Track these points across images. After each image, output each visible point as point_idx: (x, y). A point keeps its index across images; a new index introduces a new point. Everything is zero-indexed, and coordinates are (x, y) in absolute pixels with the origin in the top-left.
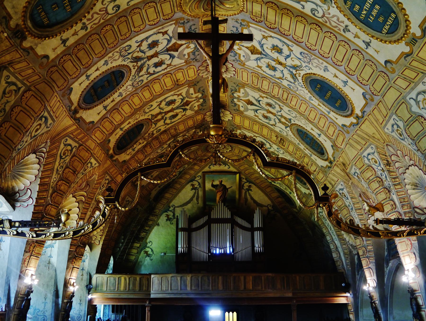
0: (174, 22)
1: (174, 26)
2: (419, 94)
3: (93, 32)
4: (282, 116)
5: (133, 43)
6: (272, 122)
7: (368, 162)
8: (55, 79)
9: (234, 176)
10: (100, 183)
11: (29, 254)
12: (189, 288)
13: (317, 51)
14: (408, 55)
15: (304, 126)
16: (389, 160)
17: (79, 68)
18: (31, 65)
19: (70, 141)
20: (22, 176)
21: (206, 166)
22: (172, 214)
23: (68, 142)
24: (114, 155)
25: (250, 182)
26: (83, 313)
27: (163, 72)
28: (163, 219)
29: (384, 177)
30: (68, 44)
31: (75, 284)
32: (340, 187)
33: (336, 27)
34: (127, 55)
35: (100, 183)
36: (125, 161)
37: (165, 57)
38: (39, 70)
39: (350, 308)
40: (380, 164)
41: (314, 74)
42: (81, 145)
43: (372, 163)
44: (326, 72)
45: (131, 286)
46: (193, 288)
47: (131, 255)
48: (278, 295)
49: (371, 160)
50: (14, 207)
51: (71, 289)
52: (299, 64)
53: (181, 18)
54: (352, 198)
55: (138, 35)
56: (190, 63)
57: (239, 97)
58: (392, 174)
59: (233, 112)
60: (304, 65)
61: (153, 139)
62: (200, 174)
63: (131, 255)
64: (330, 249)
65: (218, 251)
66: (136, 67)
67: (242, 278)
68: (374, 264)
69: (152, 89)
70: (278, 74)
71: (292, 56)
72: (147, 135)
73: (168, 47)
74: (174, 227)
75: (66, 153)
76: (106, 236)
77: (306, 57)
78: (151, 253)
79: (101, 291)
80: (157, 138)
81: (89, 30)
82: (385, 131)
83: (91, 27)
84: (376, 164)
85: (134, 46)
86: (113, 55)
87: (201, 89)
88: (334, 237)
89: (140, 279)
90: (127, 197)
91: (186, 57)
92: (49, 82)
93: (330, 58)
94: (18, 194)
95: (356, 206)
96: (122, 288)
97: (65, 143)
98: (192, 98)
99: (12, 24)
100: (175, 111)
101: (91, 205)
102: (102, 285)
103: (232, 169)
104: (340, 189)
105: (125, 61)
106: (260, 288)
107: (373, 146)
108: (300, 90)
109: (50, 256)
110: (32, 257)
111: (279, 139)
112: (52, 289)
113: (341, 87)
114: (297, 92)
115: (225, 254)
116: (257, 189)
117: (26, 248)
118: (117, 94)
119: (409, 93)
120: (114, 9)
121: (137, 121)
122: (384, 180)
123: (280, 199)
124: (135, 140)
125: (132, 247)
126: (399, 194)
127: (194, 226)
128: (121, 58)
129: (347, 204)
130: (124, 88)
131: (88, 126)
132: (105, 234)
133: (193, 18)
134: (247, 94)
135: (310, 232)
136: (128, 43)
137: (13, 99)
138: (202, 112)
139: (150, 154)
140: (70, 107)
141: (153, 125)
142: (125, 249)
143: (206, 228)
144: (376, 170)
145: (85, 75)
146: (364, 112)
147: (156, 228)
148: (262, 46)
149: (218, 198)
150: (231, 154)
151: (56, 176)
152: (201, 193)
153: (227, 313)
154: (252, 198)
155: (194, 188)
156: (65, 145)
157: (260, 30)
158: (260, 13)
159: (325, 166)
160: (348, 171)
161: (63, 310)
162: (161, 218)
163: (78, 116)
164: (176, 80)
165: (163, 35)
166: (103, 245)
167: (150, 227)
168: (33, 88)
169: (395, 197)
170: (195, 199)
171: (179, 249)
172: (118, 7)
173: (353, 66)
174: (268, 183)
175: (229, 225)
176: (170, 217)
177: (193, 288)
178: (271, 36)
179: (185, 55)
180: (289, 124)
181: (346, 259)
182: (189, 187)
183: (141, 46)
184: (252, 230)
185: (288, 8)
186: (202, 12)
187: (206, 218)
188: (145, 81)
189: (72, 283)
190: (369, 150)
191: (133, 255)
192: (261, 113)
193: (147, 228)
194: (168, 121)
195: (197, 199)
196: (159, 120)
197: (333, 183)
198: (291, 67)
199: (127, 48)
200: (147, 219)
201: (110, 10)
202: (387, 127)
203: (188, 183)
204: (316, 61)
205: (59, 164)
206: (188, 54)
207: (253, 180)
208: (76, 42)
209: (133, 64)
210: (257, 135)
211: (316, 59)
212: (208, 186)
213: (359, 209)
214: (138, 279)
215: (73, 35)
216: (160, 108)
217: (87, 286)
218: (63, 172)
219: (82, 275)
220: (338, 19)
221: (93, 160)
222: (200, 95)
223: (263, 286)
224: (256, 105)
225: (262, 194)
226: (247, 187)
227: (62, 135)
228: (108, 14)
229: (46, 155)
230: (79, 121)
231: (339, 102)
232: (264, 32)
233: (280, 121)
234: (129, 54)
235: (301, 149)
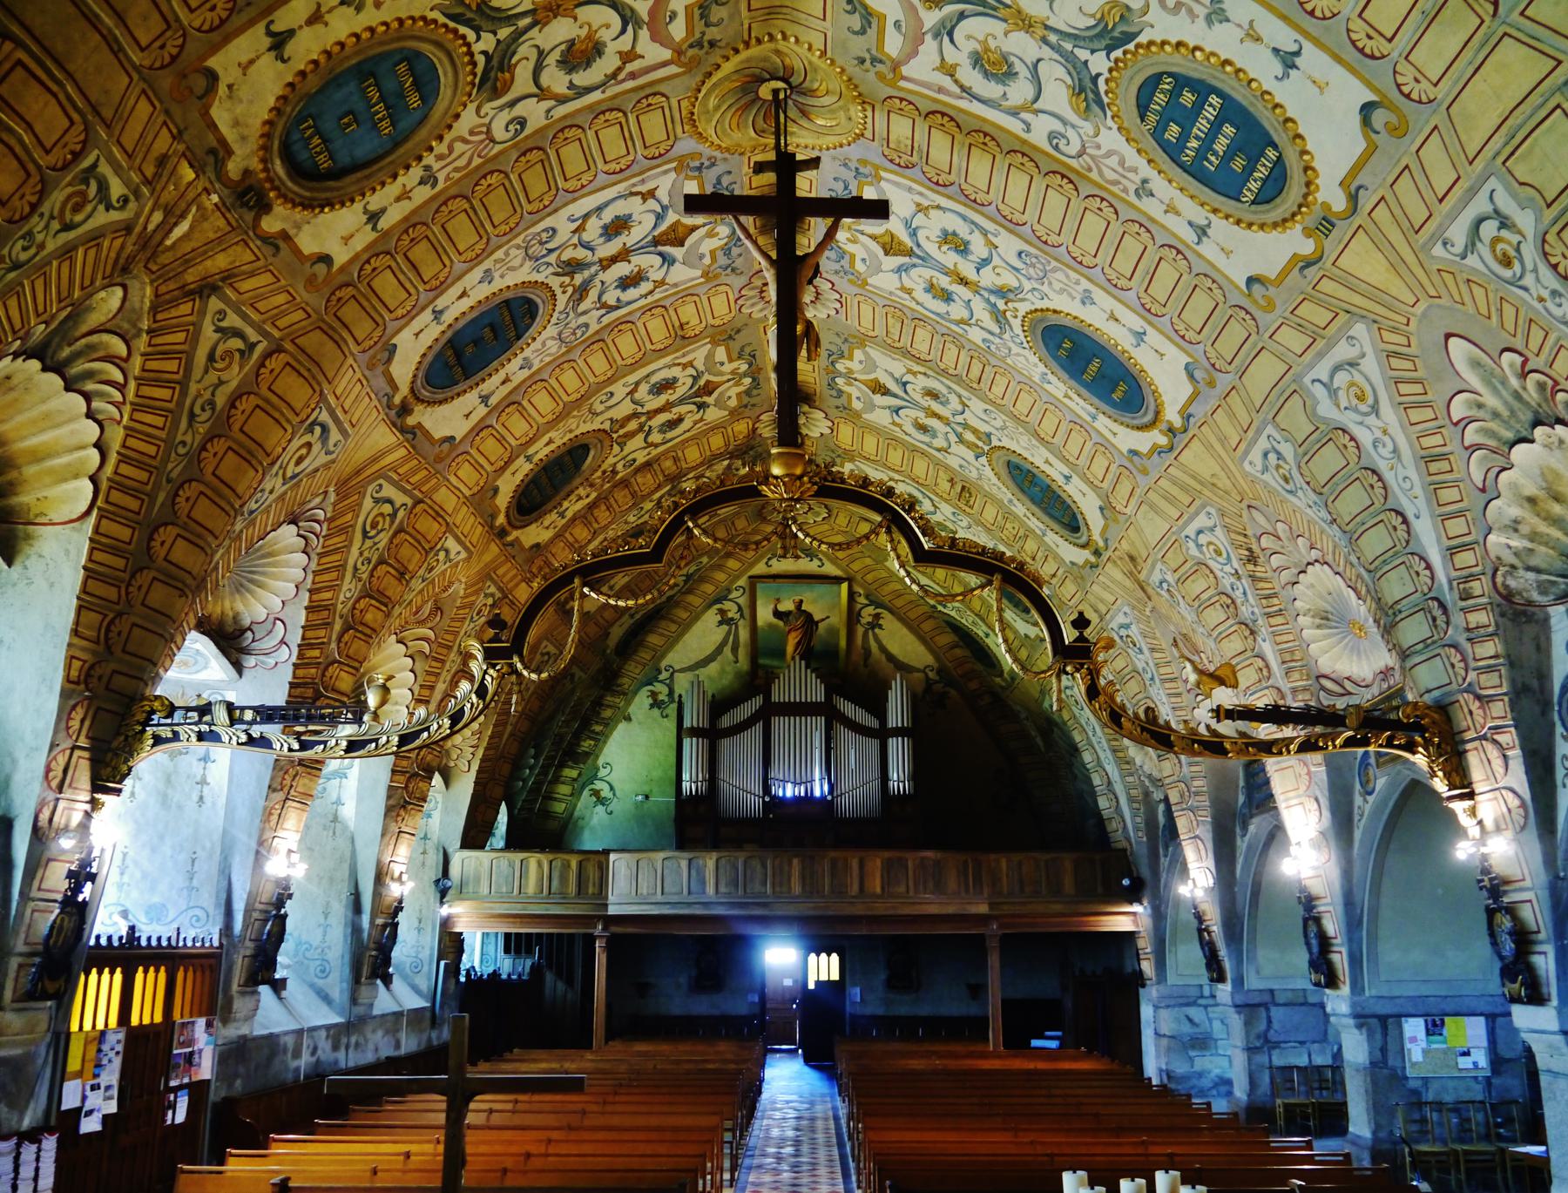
1: (673, 175)
2: (1337, 368)
3: (453, 192)
4: (966, 426)
5: (561, 222)
6: (939, 442)
7: (1197, 554)
8: (347, 320)
9: (835, 587)
10: (471, 605)
11: (280, 796)
12: (710, 890)
13: (1063, 249)
15: (1025, 454)
16: (1255, 547)
17: (412, 290)
19: (389, 491)
20: (260, 585)
21: (762, 557)
22: (665, 690)
23: (384, 494)
24: (508, 528)
25: (879, 605)
26: (427, 952)
27: (643, 302)
28: (641, 701)
29: (1238, 594)
30: (384, 223)
31: (405, 877)
32: (1121, 619)
33: (1117, 183)
35: (471, 605)
36: (537, 545)
37: (648, 261)
38: (306, 295)
39: (1141, 943)
40: (1229, 558)
41: (1055, 311)
42: (421, 501)
45: (555, 883)
46: (723, 889)
47: (556, 799)
48: (951, 910)
50: (239, 667)
51: (395, 890)
52: (1016, 284)
53: (692, 156)
54: (1152, 650)
55: (575, 200)
56: (716, 277)
57: (850, 371)
58: (1262, 585)
59: (833, 413)
60: (1027, 285)
61: (615, 486)
62: (742, 582)
63: (556, 799)
64: (1093, 787)
65: (790, 791)
66: (570, 289)
67: (855, 864)
68: (1209, 827)
69: (613, 349)
70: (957, 311)
71: (996, 261)
72: (599, 473)
73: (656, 233)
74: (671, 724)
76: (486, 749)
78: (610, 795)
79: (475, 897)
80: (625, 483)
81: (440, 186)
83: (447, 178)
84: (1219, 559)
85: (565, 229)
86: (507, 254)
87: (747, 350)
88: (1102, 756)
89: (580, 864)
90: (545, 643)
91: (707, 261)
92: (333, 329)
93: (1099, 269)
94: (249, 634)
95: (1162, 671)
96: (531, 887)
98: (722, 374)
100: (675, 410)
101: (447, 666)
102: (478, 880)
103: (830, 569)
104: (1122, 626)
106: (902, 889)
107: (1213, 511)
108: (1018, 355)
109: (339, 802)
110: (289, 803)
111: (958, 488)
112: (345, 891)
113: (1128, 347)
114: (1009, 361)
115: (808, 799)
116: (897, 625)
117: (272, 779)
118: (516, 363)
119: (1311, 366)
120: (511, 127)
121: (572, 436)
122: (1239, 601)
123: (958, 652)
124: (567, 489)
125: (557, 780)
126: (1279, 639)
127: (726, 721)
128: (528, 264)
129: (1140, 666)
130: (536, 345)
131: (437, 450)
132: (485, 744)
133: (726, 155)
134: (871, 365)
135: (1039, 741)
136: (548, 222)
137: (234, 376)
138: (747, 412)
139: (606, 527)
140: (390, 398)
141: (616, 448)
142: (538, 784)
143: (759, 727)
144: (1220, 574)
145: (430, 309)
146: (1190, 416)
147: (622, 727)
148: (914, 234)
149: (790, 649)
150: (826, 527)
151: (352, 586)
152: (744, 634)
153: (813, 956)
154: (883, 649)
155: (725, 620)
156: (377, 501)
157: (910, 190)
159: (1080, 562)
160: (1142, 577)
161: (372, 945)
162: (637, 699)
163: (411, 421)
164: (677, 324)
165: (645, 200)
166: (479, 772)
167: (606, 725)
168: (288, 346)
169: (1267, 648)
170: (727, 650)
171: (686, 785)
172: (522, 122)
173: (1160, 289)
174: (926, 609)
175: (821, 721)
176: (661, 697)
177: (723, 889)
178: (938, 207)
179: (702, 257)
180: (986, 448)
181: (1134, 816)
182: (711, 617)
184: (882, 734)
185: (987, 129)
186: (751, 139)
187: (758, 701)
188: (594, 327)
189: (396, 874)
190: (1201, 521)
191: (560, 801)
192: (909, 414)
193: (598, 728)
194: (656, 437)
195: (735, 650)
196: (631, 435)
197: (1103, 609)
198: (991, 292)
199: (544, 235)
200: (598, 704)
201: (499, 132)
202: (1250, 458)
203: (710, 606)
204: (1059, 275)
205: (361, 554)
206: (712, 253)
207: (886, 600)
208: (406, 219)
210: (897, 477)
212: (764, 615)
213: (1172, 680)
214: (574, 864)
215: (398, 199)
216: (634, 402)
217: (437, 882)
218: (372, 575)
219: (424, 853)
220: (1122, 163)
221: (451, 543)
222: (744, 367)
223: (911, 883)
224: (895, 396)
225: (910, 638)
226: (870, 619)
227: (369, 472)
228: (493, 141)
229: (325, 526)
230: (415, 434)
231: (1122, 387)
232: (921, 194)
233: (961, 440)
234: (550, 251)
235: (1016, 517)
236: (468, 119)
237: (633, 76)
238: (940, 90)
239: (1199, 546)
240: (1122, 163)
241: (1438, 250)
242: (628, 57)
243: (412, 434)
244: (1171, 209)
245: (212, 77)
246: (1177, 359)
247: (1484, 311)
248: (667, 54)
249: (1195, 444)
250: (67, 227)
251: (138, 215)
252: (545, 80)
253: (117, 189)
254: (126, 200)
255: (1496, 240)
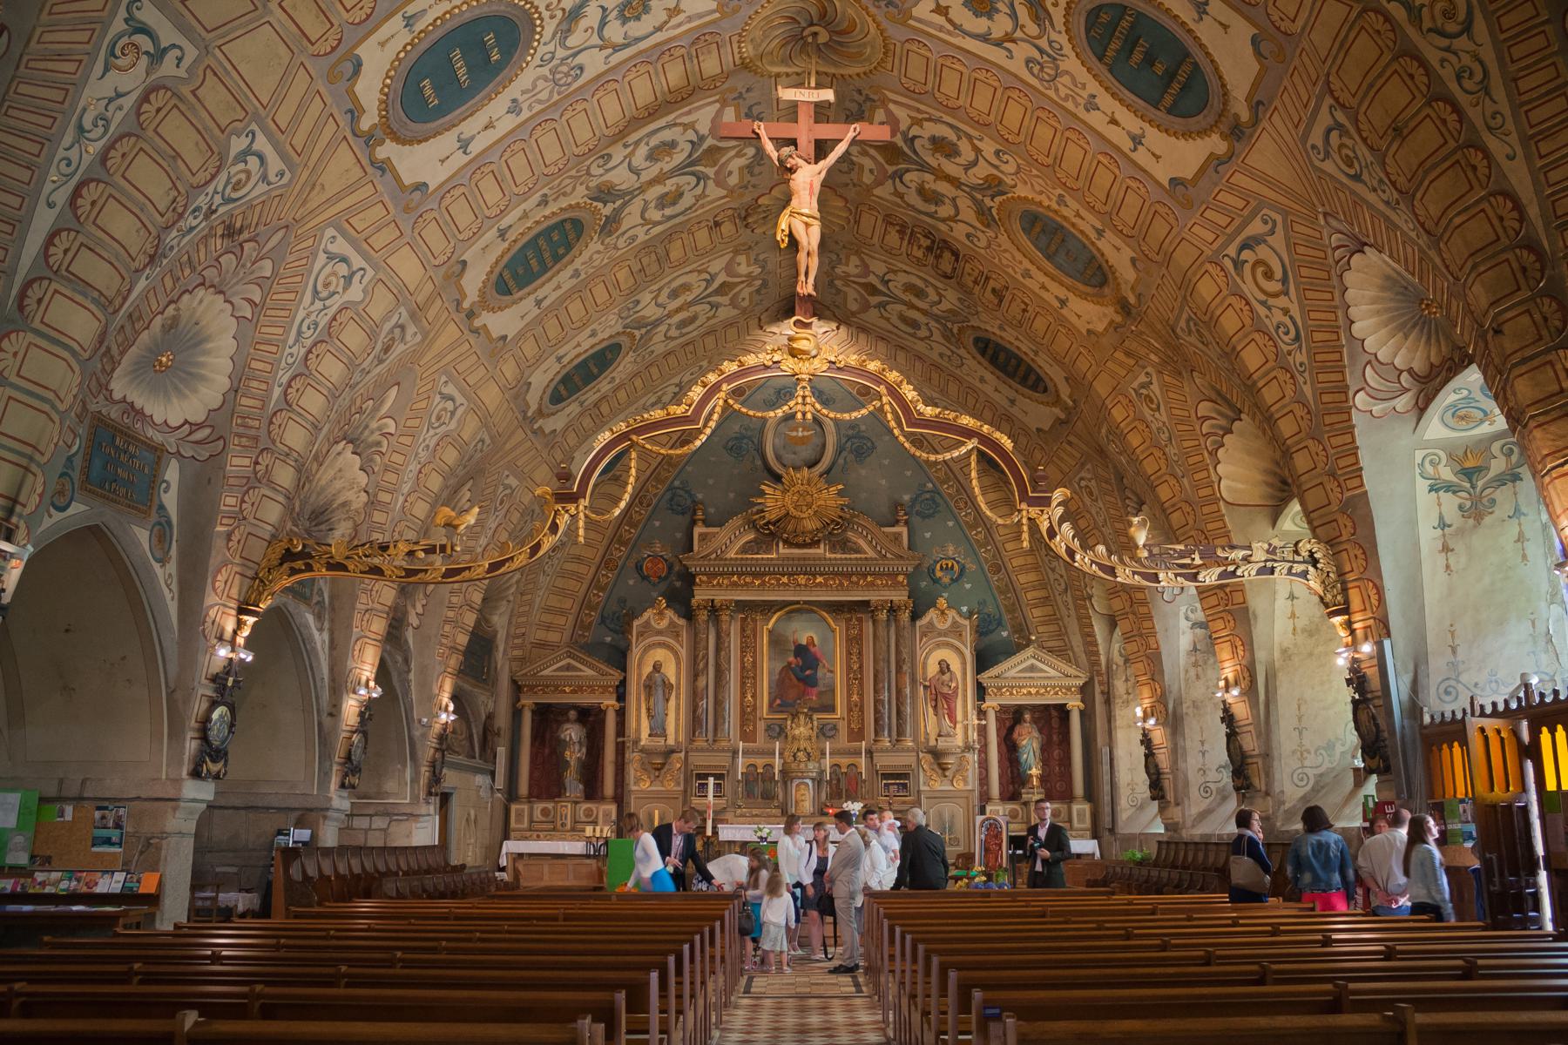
0: (911, 22)
1: (916, 12)
5: (1016, 60)
7: (233, 152)
14: (459, 303)
18: (1154, 291)
34: (1049, 56)
42: (1328, 83)
43: (233, 170)
44: (510, 104)
49: (241, 166)
52: (569, 43)
58: (202, 247)
60: (561, 53)
75: (1347, 156)
77: (567, 75)
82: (329, 225)
85: (1022, 51)
86: (1066, 99)
97: (1321, 156)
99: (1118, 319)
105: (1061, 49)
122: (181, 223)
144: (210, 189)
145: (1133, 156)
146: (383, 170)
156: (1327, 155)
158: (701, 59)
163: (1245, 116)
169: (142, 284)
172: (997, 153)
173: (488, 185)
178: (659, 29)
183: (1007, 34)
190: (275, 163)
199: (1036, 72)
204: (544, 96)
205: (1375, 190)
209: (1051, 9)
211: (548, 100)
228: (1018, 166)
230: (1259, 103)
232: (679, 25)
234: (1041, 51)
236: (1022, 191)
237: (919, 111)
238: (689, 112)
239: (243, 156)
240: (565, 194)
241: (444, 379)
242: (917, 122)
243: (1257, 106)
244: (525, 215)
245: (1088, 331)
246: (435, 177)
247: (414, 407)
248: (892, 106)
249: (358, 172)
250: (1158, 409)
251: (1153, 367)
252: (971, 156)
253: (1142, 379)
254: (1147, 373)
255: (445, 409)
